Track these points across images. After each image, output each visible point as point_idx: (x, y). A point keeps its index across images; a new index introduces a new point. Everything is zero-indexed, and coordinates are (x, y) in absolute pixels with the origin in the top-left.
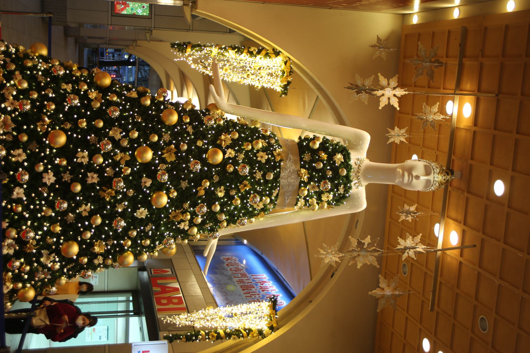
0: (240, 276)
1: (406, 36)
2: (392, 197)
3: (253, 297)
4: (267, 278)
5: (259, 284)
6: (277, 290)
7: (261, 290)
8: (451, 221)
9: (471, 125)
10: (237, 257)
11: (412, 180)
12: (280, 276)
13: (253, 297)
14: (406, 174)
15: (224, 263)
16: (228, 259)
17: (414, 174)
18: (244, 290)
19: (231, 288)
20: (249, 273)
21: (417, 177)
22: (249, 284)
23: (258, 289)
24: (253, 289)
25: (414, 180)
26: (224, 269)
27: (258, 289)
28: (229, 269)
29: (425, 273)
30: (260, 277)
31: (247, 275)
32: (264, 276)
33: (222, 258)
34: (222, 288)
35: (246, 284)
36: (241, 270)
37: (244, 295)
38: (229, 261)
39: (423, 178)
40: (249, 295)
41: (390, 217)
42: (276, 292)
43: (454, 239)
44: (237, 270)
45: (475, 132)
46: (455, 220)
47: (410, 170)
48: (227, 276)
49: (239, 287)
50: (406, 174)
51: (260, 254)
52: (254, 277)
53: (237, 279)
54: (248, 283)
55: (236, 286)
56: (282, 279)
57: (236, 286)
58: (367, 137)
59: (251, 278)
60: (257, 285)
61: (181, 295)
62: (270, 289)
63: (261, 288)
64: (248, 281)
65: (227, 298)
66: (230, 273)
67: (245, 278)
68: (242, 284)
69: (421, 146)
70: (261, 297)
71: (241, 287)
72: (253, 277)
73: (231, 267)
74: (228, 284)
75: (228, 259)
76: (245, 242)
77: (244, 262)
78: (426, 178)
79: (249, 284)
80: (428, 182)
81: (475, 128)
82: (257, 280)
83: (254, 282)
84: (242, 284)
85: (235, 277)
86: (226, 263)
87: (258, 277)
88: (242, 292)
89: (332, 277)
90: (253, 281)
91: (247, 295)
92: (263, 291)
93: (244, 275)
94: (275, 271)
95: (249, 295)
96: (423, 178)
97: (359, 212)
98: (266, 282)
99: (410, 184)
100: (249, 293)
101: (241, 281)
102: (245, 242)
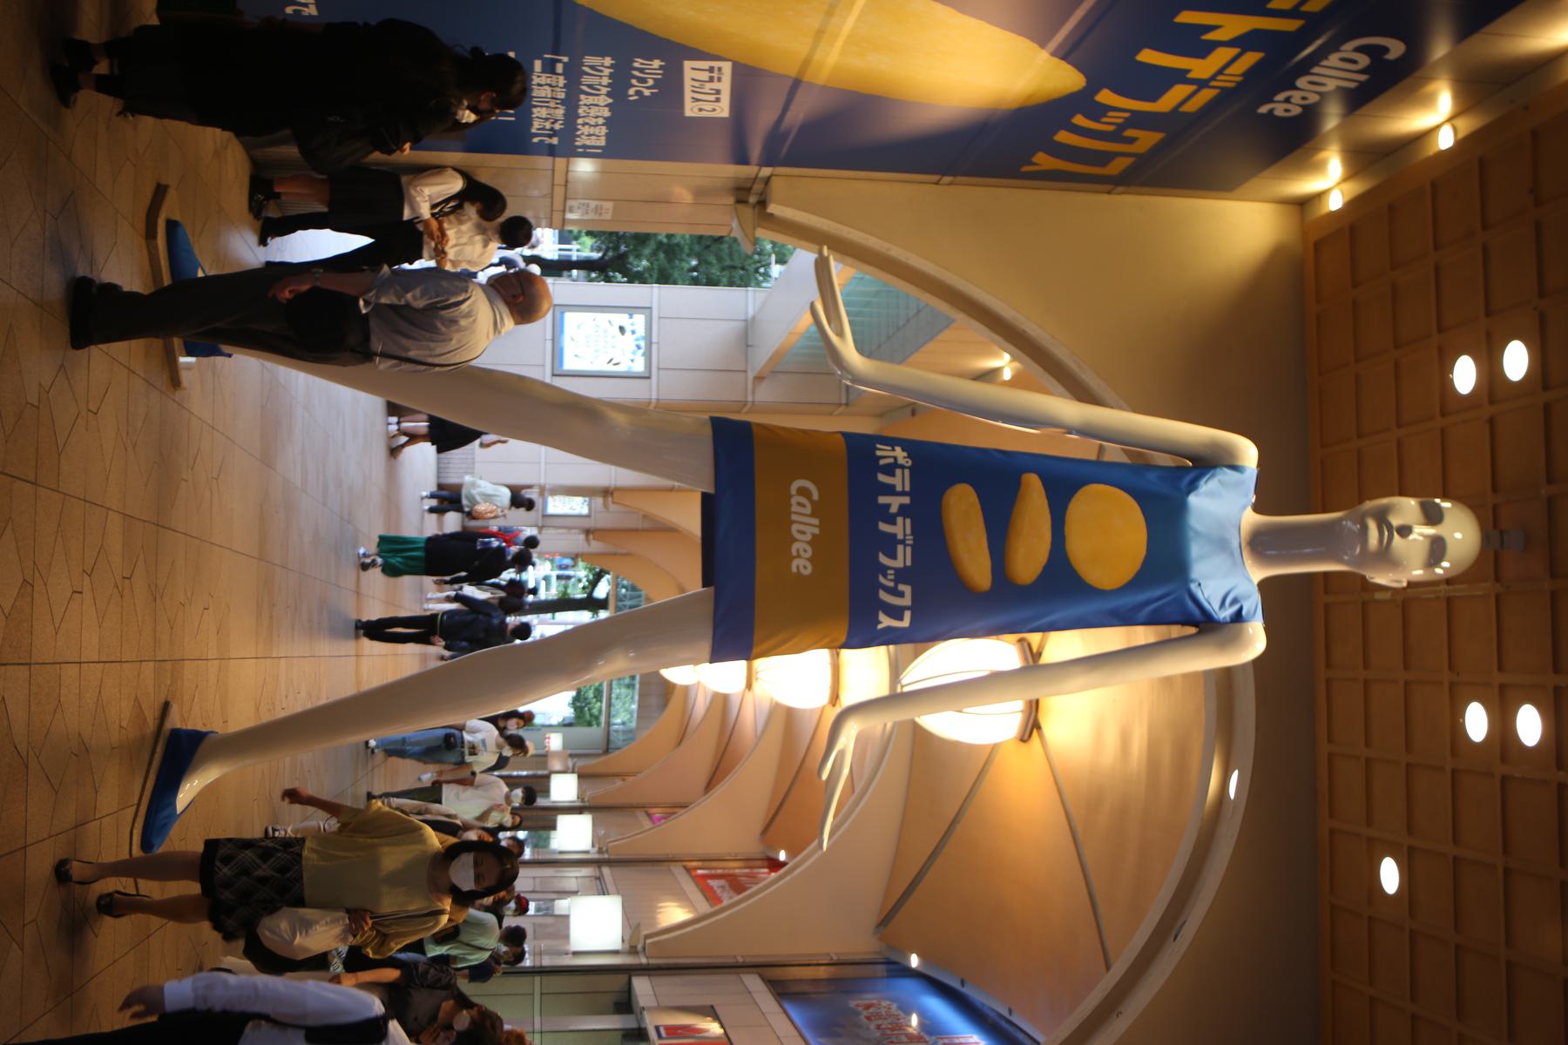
1: (1317, 246)
2: (1329, 682)
12: (1021, 1036)
14: (1372, 526)
15: (858, 1014)
16: (868, 1007)
17: (1396, 521)
20: (930, 1033)
21: (1405, 531)
28: (872, 1027)
29: (1456, 859)
33: (852, 1004)
39: (1421, 532)
41: (1330, 741)
43: (1530, 725)
45: (1547, 408)
47: (1382, 517)
50: (1372, 526)
51: (956, 984)
58: (1248, 452)
66: (878, 1034)
76: (914, 961)
77: (914, 1020)
78: (1430, 531)
80: (1437, 549)
86: (865, 1013)
94: (1003, 1024)
96: (1421, 532)
97: (1244, 666)
99: (1385, 556)
102: (914, 961)
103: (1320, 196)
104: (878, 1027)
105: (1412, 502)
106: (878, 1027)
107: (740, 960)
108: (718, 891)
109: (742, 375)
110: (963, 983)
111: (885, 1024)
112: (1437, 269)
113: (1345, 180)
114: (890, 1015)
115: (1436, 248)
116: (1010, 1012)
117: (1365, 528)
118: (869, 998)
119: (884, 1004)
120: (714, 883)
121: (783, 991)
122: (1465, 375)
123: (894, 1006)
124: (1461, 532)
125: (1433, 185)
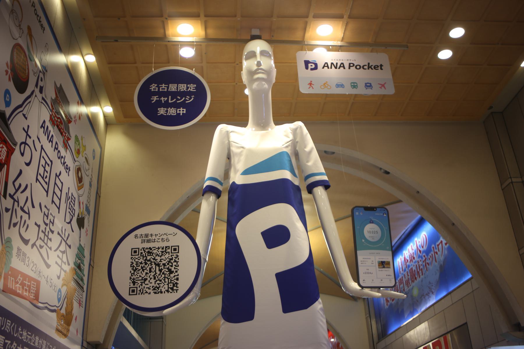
0: (402, 285)
1: (125, 117)
3: (421, 267)
4: (401, 257)
5: (407, 264)
6: (411, 244)
7: (414, 261)
8: (308, 35)
9: (200, 21)
11: (262, 69)
13: (421, 267)
14: (256, 76)
15: (391, 304)
16: (387, 301)
17: (255, 68)
18: (416, 278)
19: (415, 292)
22: (409, 274)
23: (413, 264)
24: (414, 268)
25: (261, 67)
26: (397, 303)
27: (413, 264)
30: (400, 264)
31: (400, 278)
33: (386, 307)
34: (417, 301)
35: (409, 277)
37: (421, 277)
38: (389, 299)
40: (420, 272)
42: (414, 244)
46: (305, 30)
49: (413, 284)
52: (401, 270)
53: (406, 288)
54: (408, 275)
55: (413, 287)
57: (413, 287)
58: (222, 128)
59: (402, 274)
60: (409, 266)
61: (430, 344)
62: (411, 252)
63: (411, 261)
64: (406, 276)
65: (427, 295)
67: (404, 279)
68: (410, 281)
69: (234, 84)
70: (420, 259)
71: (413, 281)
74: (412, 296)
79: (409, 274)
81: (202, 15)
84: (410, 281)
85: (404, 290)
87: (401, 266)
90: (405, 270)
91: (421, 274)
92: (414, 258)
95: (420, 272)
98: (405, 258)
100: (418, 272)
101: (407, 283)
103: (105, 116)
105: (245, 64)
112: (143, 63)
113: (100, 105)
115: (135, 63)
117: (258, 79)
121: (383, 334)
122: (187, 53)
124: (258, 46)
125: (109, 63)
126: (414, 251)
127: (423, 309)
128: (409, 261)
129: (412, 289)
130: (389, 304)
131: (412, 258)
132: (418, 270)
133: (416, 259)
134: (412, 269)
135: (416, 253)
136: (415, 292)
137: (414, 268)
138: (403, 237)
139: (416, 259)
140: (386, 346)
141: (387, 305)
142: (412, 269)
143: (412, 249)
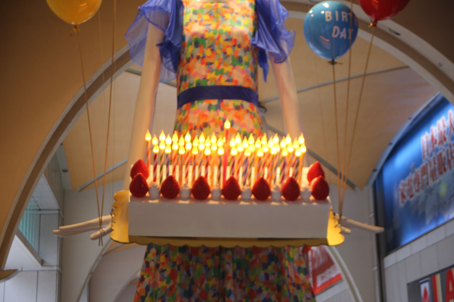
0: (425, 177)
7: (445, 143)
10: (399, 182)
12: (423, 114)
16: (403, 196)
18: (445, 170)
19: (443, 190)
24: (444, 154)
26: (417, 201)
27: (442, 147)
28: (417, 194)
30: (425, 145)
31: (424, 164)
32: (424, 139)
33: (402, 205)
35: (437, 166)
36: (417, 176)
38: (406, 194)
40: (452, 161)
42: (447, 118)
44: (417, 180)
48: (426, 197)
49: (441, 178)
51: (390, 148)
52: (426, 153)
53: (431, 181)
54: (435, 163)
56: (427, 110)
59: (427, 160)
60: (437, 150)
63: (441, 142)
64: (432, 163)
68: (437, 173)
71: (441, 173)
72: (426, 157)
73: (414, 190)
74: (438, 195)
75: (403, 196)
79: (436, 161)
82: (431, 150)
83: (434, 155)
84: (437, 173)
85: (428, 183)
86: (408, 198)
87: (425, 148)
88: (449, 171)
89: (398, 34)
90: (431, 155)
92: (445, 139)
93: (424, 171)
100: (449, 162)
101: (433, 174)
104: (418, 191)
106: (418, 191)
107: (376, 268)
108: (325, 280)
109: (40, 273)
110: (390, 144)
111: (415, 187)
114: (409, 184)
116: (410, 118)
118: (397, 196)
119: (401, 187)
120: (320, 282)
123: (402, 182)
126: (446, 129)
127: (451, 216)
128: (438, 142)
129: (439, 183)
130: (405, 201)
131: (443, 139)
132: (450, 158)
133: (448, 141)
134: (441, 154)
135: (448, 131)
136: (443, 190)
137: (444, 154)
138: (432, 105)
139: (448, 141)
140: (397, 263)
141: (403, 202)
142: (441, 154)
143: (444, 126)
